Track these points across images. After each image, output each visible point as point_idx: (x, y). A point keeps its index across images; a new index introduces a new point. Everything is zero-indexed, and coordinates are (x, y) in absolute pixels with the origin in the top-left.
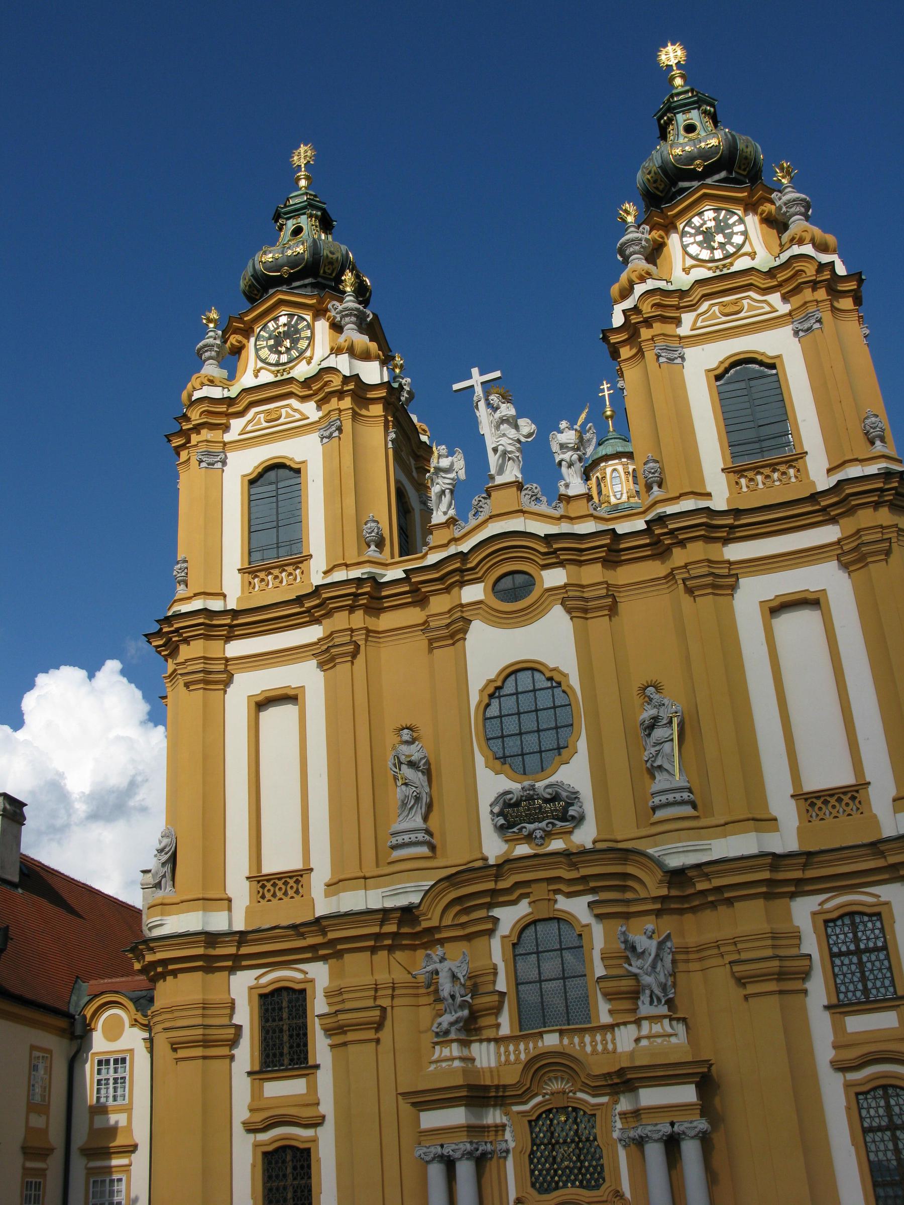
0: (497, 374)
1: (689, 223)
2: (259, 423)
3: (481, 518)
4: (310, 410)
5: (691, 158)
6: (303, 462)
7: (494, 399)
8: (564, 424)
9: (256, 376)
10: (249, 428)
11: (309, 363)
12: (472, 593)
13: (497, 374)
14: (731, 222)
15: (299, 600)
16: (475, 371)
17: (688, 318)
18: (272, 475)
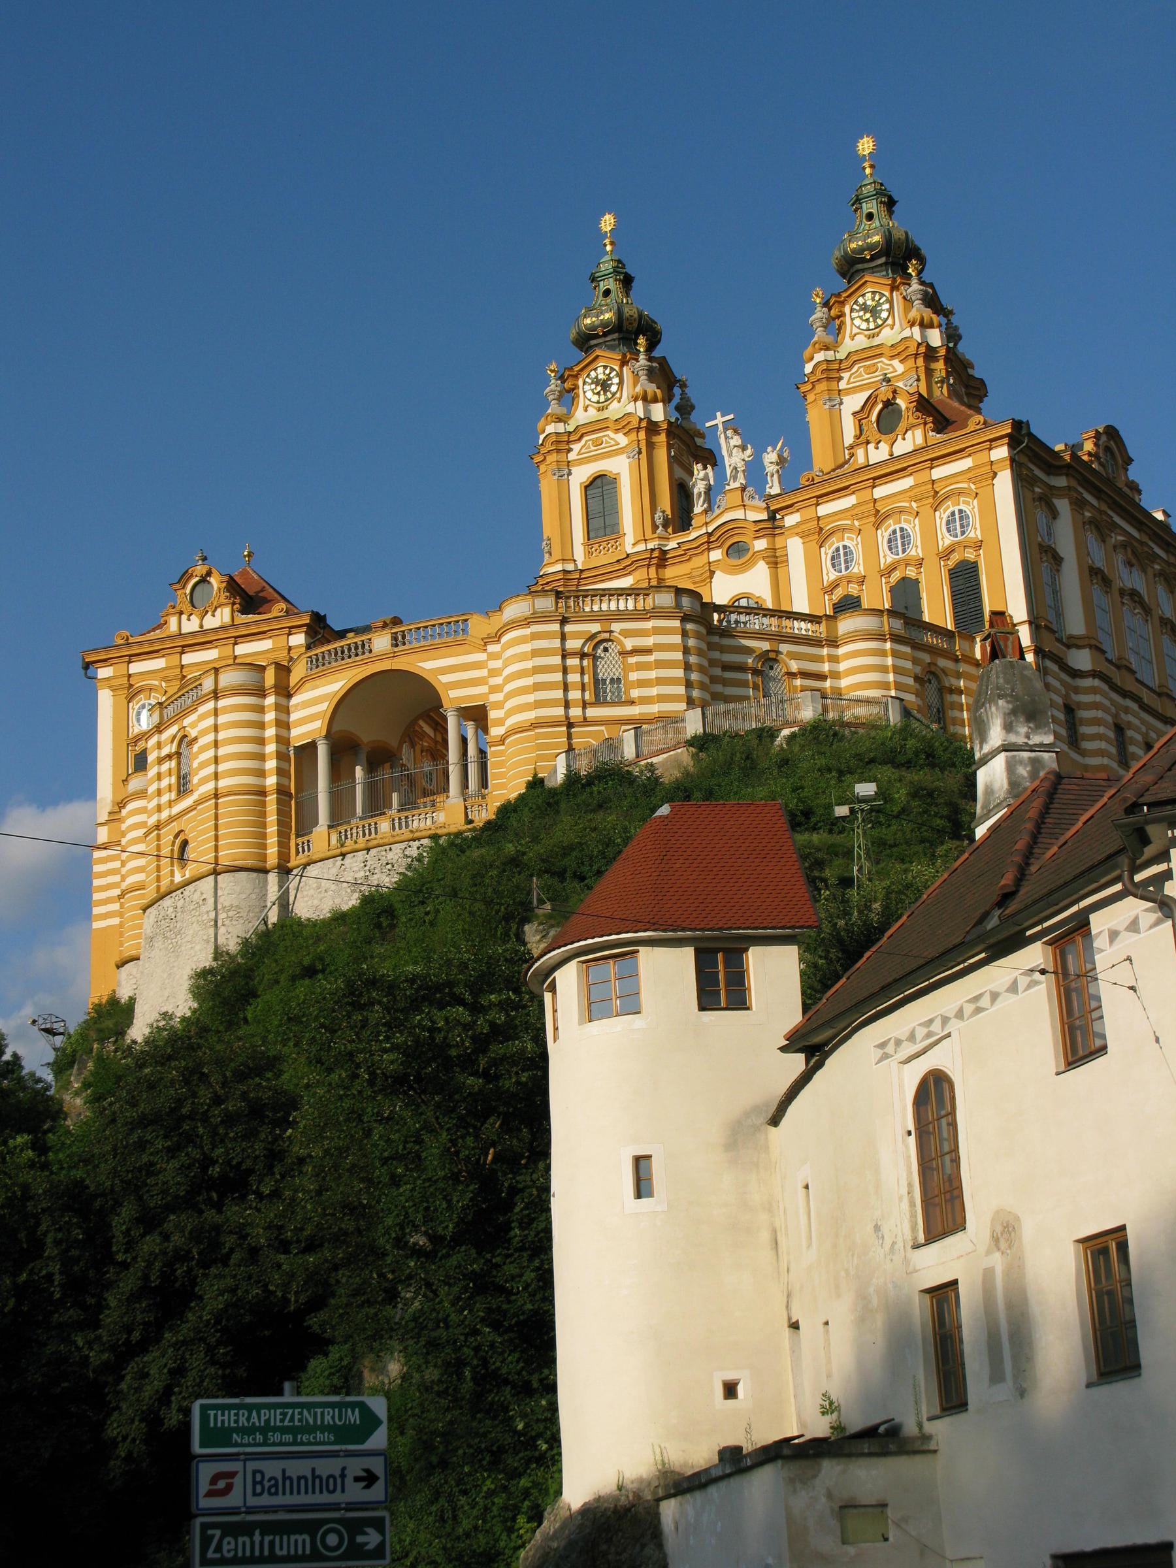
0: (731, 416)
1: (856, 302)
2: (589, 447)
3: (722, 509)
4: (622, 440)
5: (861, 250)
6: (618, 474)
7: (729, 433)
8: (769, 449)
9: (586, 411)
10: (583, 451)
11: (619, 402)
12: (716, 555)
13: (731, 416)
14: (881, 301)
15: (618, 561)
16: (718, 414)
17: (846, 375)
18: (599, 481)
